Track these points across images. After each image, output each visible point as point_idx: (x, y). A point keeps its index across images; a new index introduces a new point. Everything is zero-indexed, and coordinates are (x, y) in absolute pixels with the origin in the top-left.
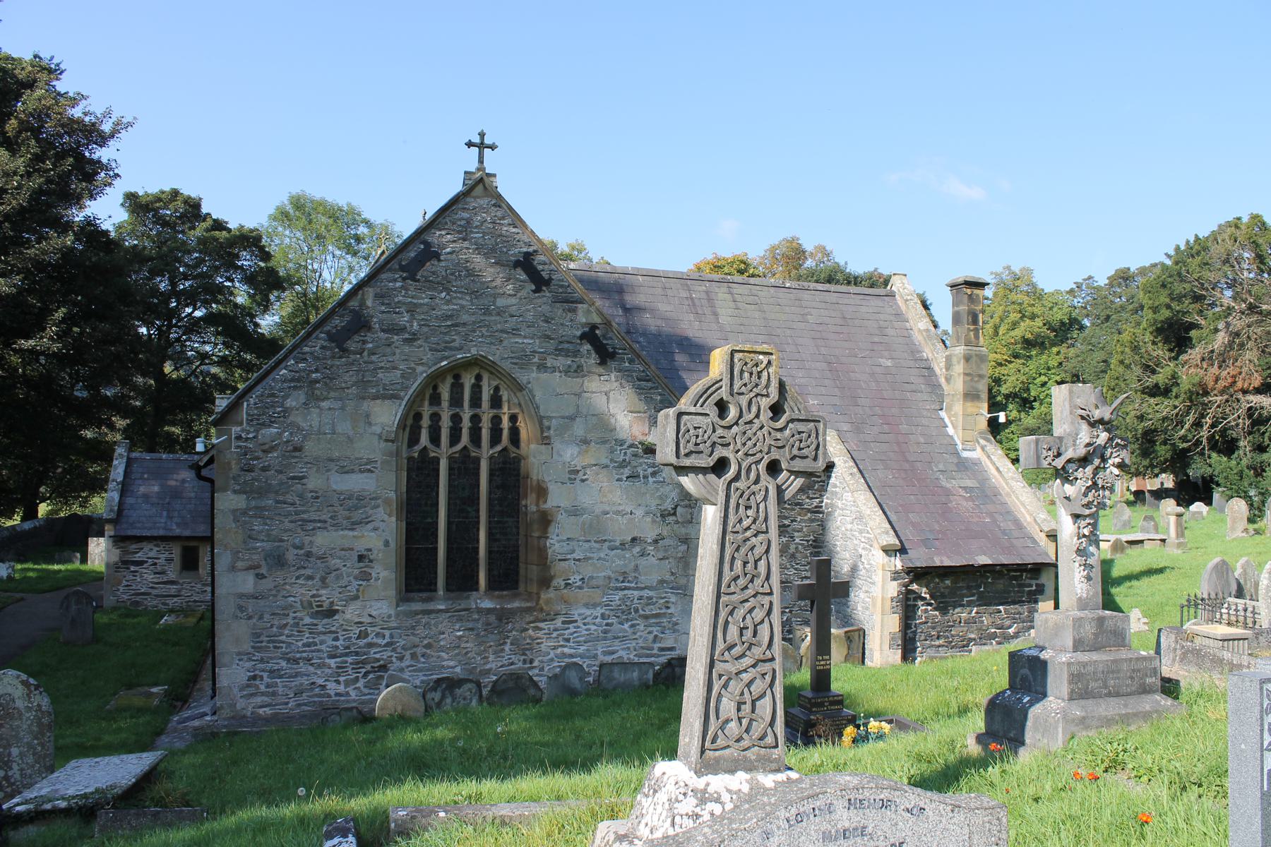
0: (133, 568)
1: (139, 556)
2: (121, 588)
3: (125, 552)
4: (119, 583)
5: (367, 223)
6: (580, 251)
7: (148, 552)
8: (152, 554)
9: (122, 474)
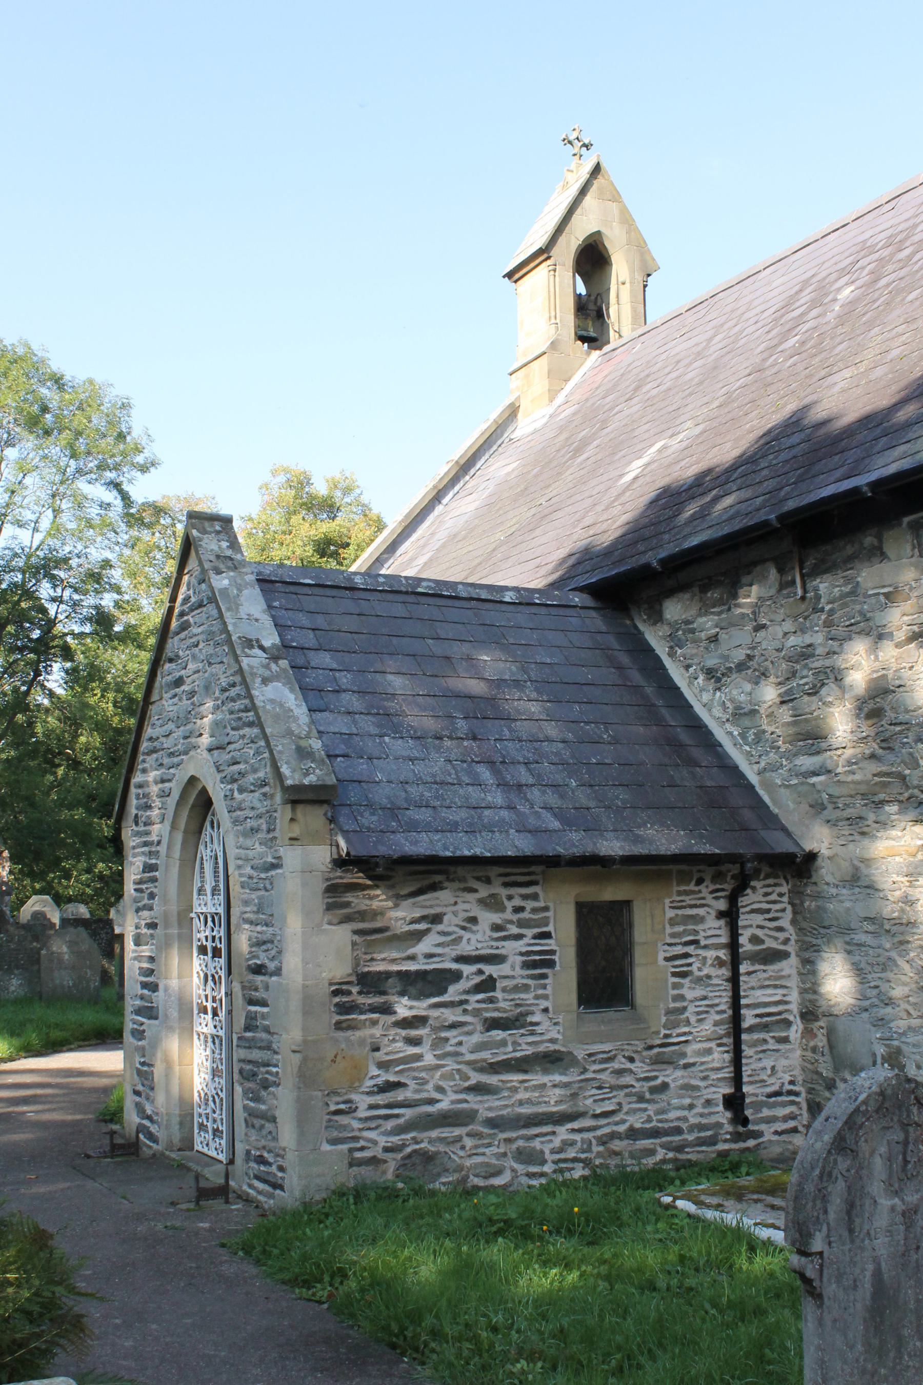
0: (404, 1008)
1: (428, 953)
2: (362, 1102)
3: (372, 934)
4: (357, 1074)
5: (58, 381)
6: (347, 491)
7: (460, 928)
8: (477, 941)
9: (267, 621)
